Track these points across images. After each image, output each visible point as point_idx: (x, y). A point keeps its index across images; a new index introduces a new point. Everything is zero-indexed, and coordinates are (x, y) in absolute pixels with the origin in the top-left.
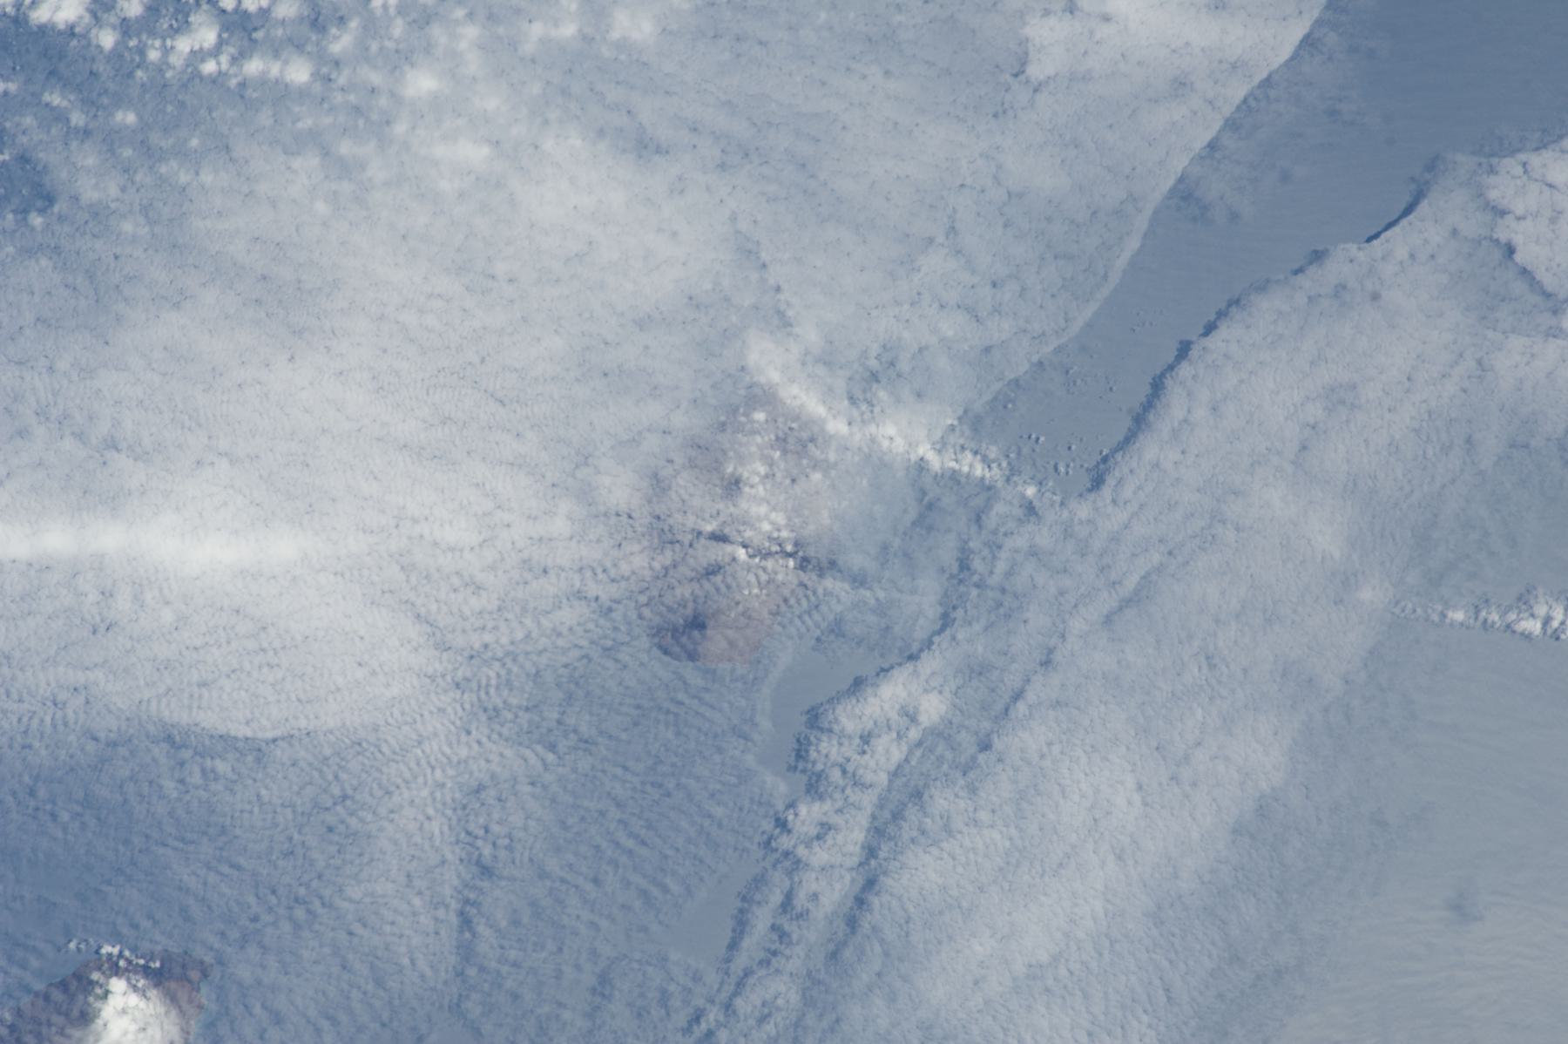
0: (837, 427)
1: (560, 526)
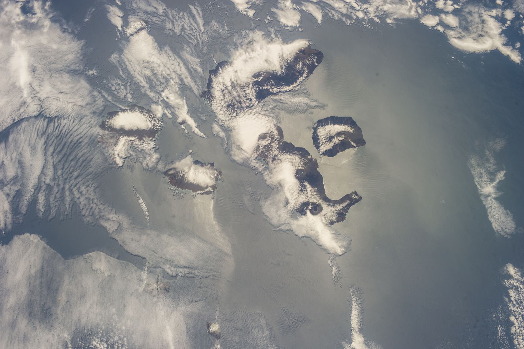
0: (145, 282)
1: (160, 304)
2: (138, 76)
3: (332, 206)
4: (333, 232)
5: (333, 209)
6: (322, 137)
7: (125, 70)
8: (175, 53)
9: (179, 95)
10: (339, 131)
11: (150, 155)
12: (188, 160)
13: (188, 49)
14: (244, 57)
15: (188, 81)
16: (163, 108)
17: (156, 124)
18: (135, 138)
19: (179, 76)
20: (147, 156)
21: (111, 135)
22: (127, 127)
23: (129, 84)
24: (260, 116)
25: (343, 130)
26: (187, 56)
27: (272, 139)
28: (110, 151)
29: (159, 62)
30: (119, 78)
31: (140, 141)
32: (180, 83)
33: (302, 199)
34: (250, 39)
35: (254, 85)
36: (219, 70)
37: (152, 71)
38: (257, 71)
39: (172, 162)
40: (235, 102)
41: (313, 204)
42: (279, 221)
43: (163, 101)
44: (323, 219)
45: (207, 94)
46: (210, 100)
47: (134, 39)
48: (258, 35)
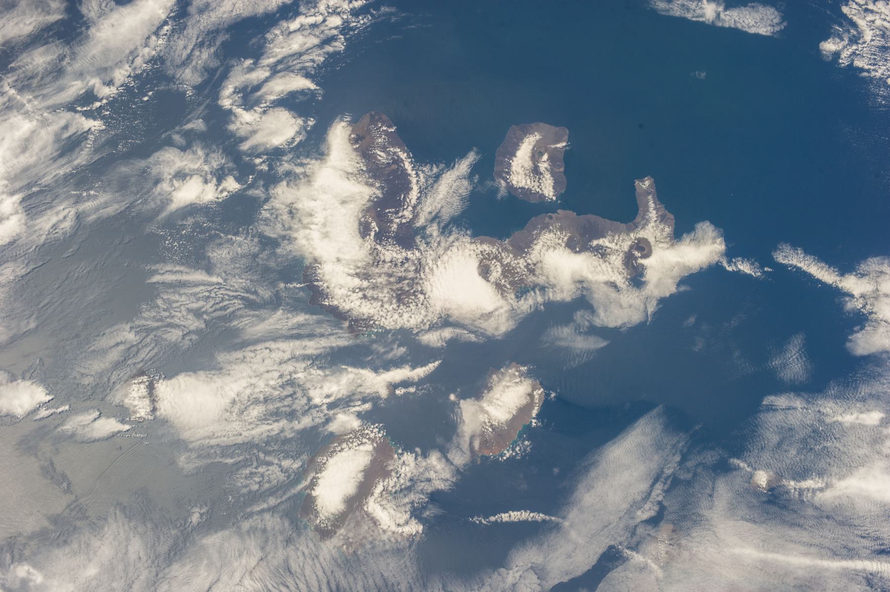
2: (254, 432)
3: (646, 224)
4: (688, 240)
5: (652, 224)
6: (529, 182)
7: (226, 450)
8: (241, 349)
9: (333, 373)
10: (529, 154)
11: (427, 469)
12: (467, 408)
13: (246, 321)
14: (315, 234)
15: (312, 347)
16: (345, 412)
17: (372, 435)
18: (381, 484)
19: (294, 358)
20: (427, 475)
21: (352, 525)
22: (350, 489)
23: (262, 455)
24: (445, 258)
25: (531, 147)
26: (261, 328)
27: (496, 257)
28: (385, 537)
29: (244, 383)
30: (238, 470)
31: (391, 476)
32: (309, 363)
33: (617, 260)
34: (284, 210)
35: (381, 241)
36: (318, 286)
37: (256, 402)
38: (356, 225)
39: (458, 435)
40: (401, 285)
41: (631, 247)
42: (638, 310)
43: (331, 406)
44: (661, 245)
45: (357, 324)
46: (372, 326)
47: (165, 408)
48: (283, 193)
